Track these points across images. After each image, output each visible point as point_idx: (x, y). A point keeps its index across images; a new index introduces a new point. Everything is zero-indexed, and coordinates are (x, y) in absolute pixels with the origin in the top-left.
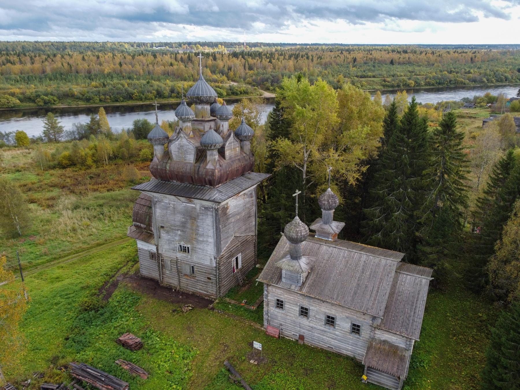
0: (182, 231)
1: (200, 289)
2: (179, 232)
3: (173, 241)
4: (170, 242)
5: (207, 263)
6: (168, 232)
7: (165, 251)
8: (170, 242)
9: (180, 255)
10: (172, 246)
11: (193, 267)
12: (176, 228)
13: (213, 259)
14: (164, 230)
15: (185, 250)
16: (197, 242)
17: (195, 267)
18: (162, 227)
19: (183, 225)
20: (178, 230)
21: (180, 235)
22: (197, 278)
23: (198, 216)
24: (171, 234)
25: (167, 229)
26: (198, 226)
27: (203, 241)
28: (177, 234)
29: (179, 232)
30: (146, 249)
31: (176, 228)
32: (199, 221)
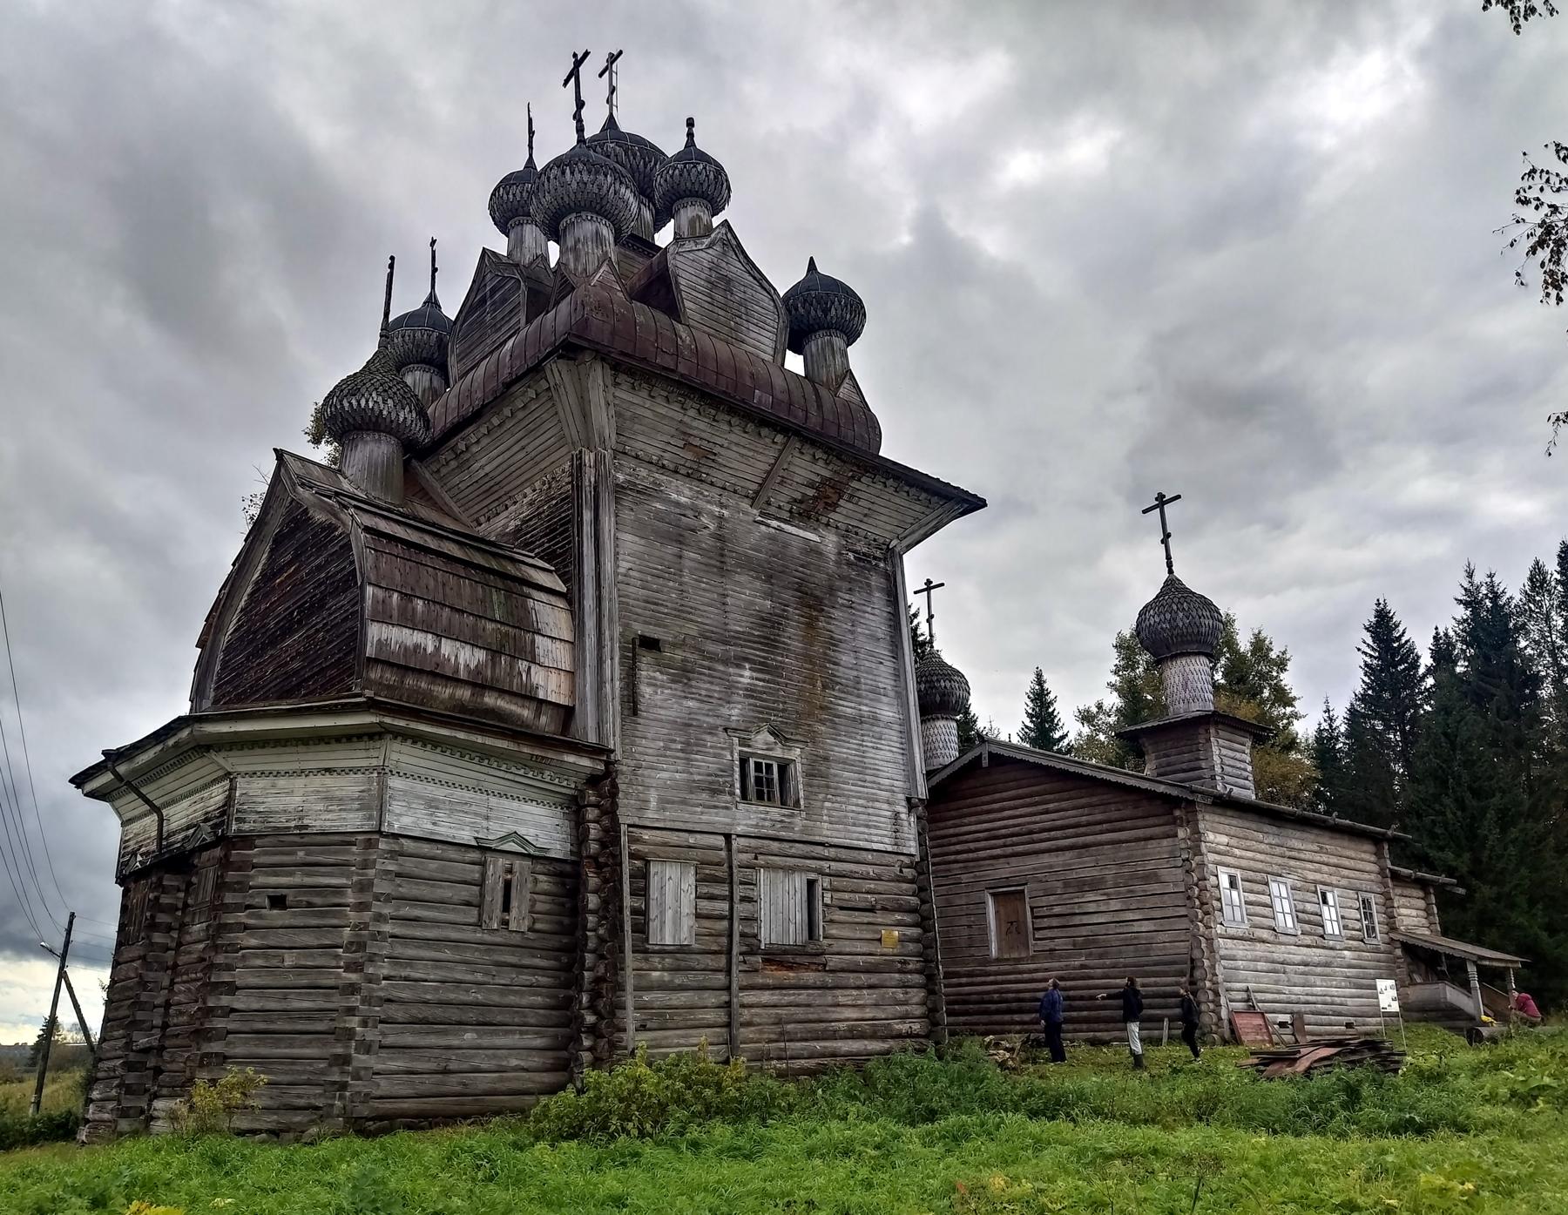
0: (762, 667)
1: (853, 1034)
2: (746, 676)
3: (712, 730)
4: (689, 736)
5: (881, 840)
6: (683, 675)
7: (664, 802)
8: (689, 736)
9: (748, 818)
10: (705, 764)
11: (811, 884)
12: (733, 650)
13: (902, 809)
14: (661, 666)
15: (766, 784)
16: (834, 725)
17: (824, 882)
18: (651, 644)
19: (769, 630)
20: (739, 661)
21: (751, 692)
22: (834, 961)
23: (832, 590)
24: (703, 687)
25: (679, 655)
26: (833, 643)
27: (859, 720)
28: (731, 687)
29: (746, 676)
30: (466, 836)
31: (733, 650)
32: (836, 613)
